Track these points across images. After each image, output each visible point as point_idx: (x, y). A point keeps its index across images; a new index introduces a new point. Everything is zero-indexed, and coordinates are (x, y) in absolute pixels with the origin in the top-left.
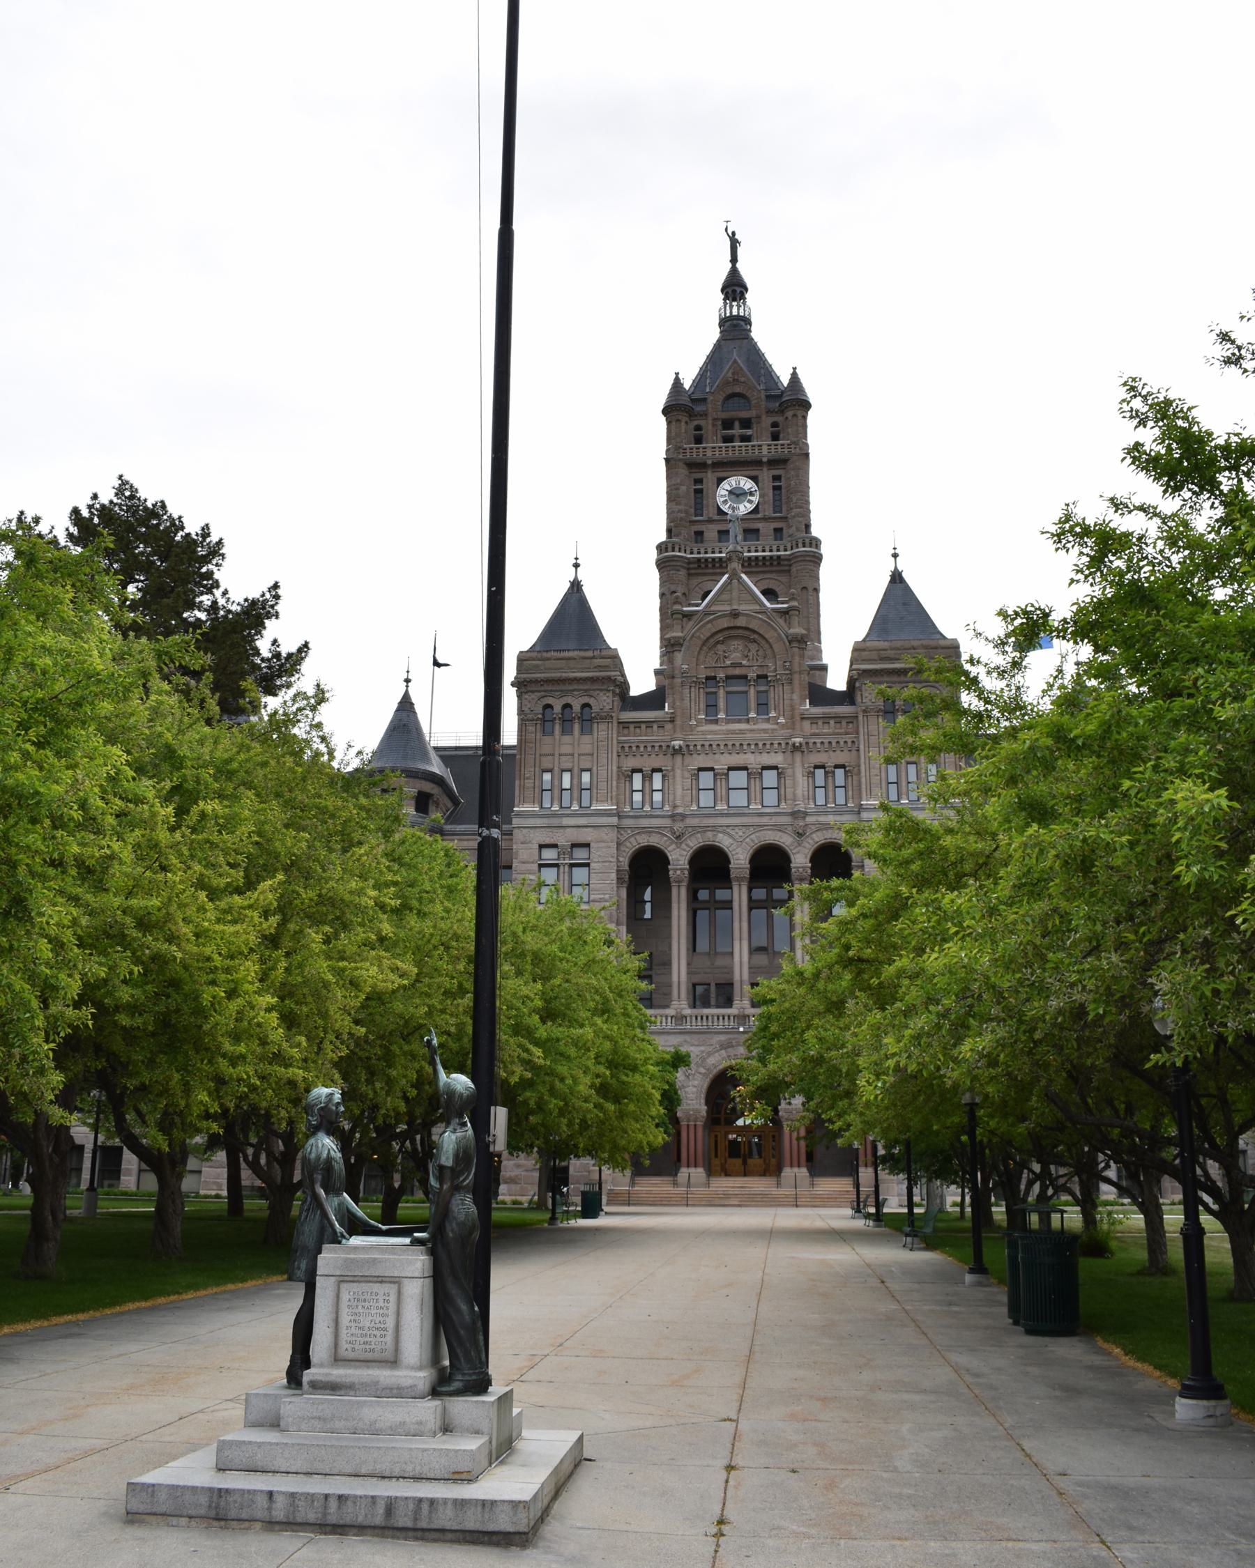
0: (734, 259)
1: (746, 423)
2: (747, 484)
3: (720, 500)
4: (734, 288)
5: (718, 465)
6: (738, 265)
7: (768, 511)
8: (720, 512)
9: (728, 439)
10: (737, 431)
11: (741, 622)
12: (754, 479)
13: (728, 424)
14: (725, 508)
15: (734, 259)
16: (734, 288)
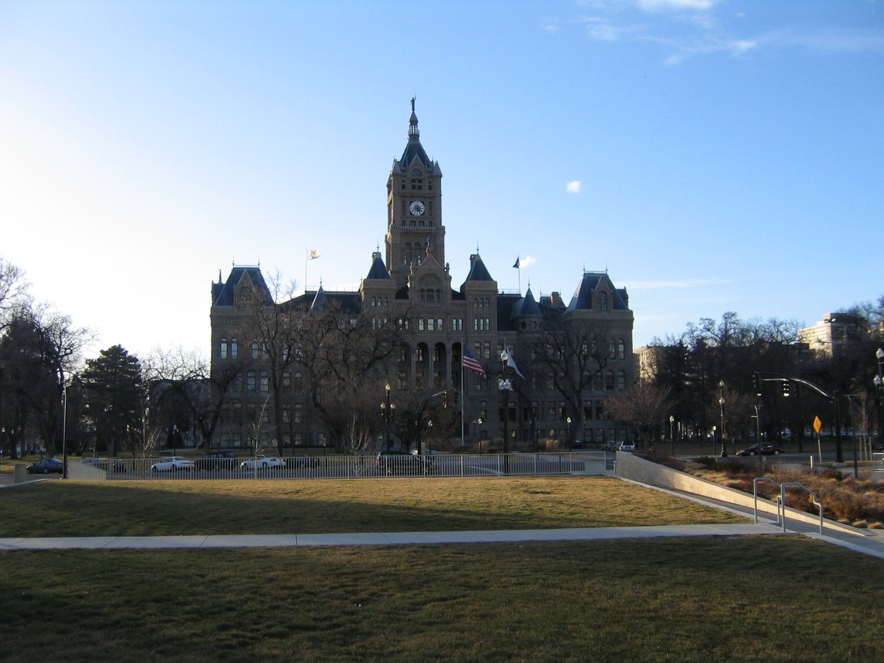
0: (413, 109)
1: (420, 181)
2: (420, 204)
3: (411, 210)
4: (414, 122)
5: (411, 196)
6: (415, 112)
7: (427, 215)
8: (411, 214)
9: (414, 187)
10: (417, 184)
11: (432, 272)
12: (423, 203)
13: (413, 181)
14: (413, 213)
15: (413, 109)
16: (414, 122)
